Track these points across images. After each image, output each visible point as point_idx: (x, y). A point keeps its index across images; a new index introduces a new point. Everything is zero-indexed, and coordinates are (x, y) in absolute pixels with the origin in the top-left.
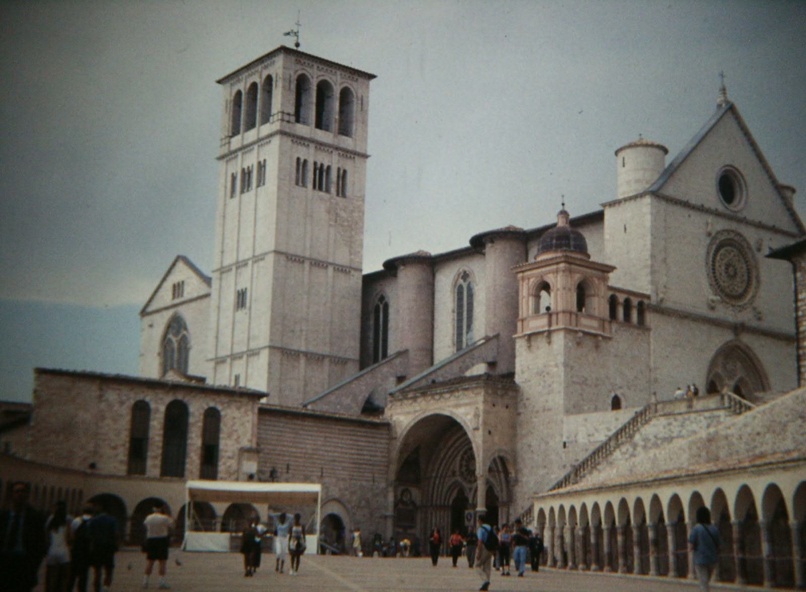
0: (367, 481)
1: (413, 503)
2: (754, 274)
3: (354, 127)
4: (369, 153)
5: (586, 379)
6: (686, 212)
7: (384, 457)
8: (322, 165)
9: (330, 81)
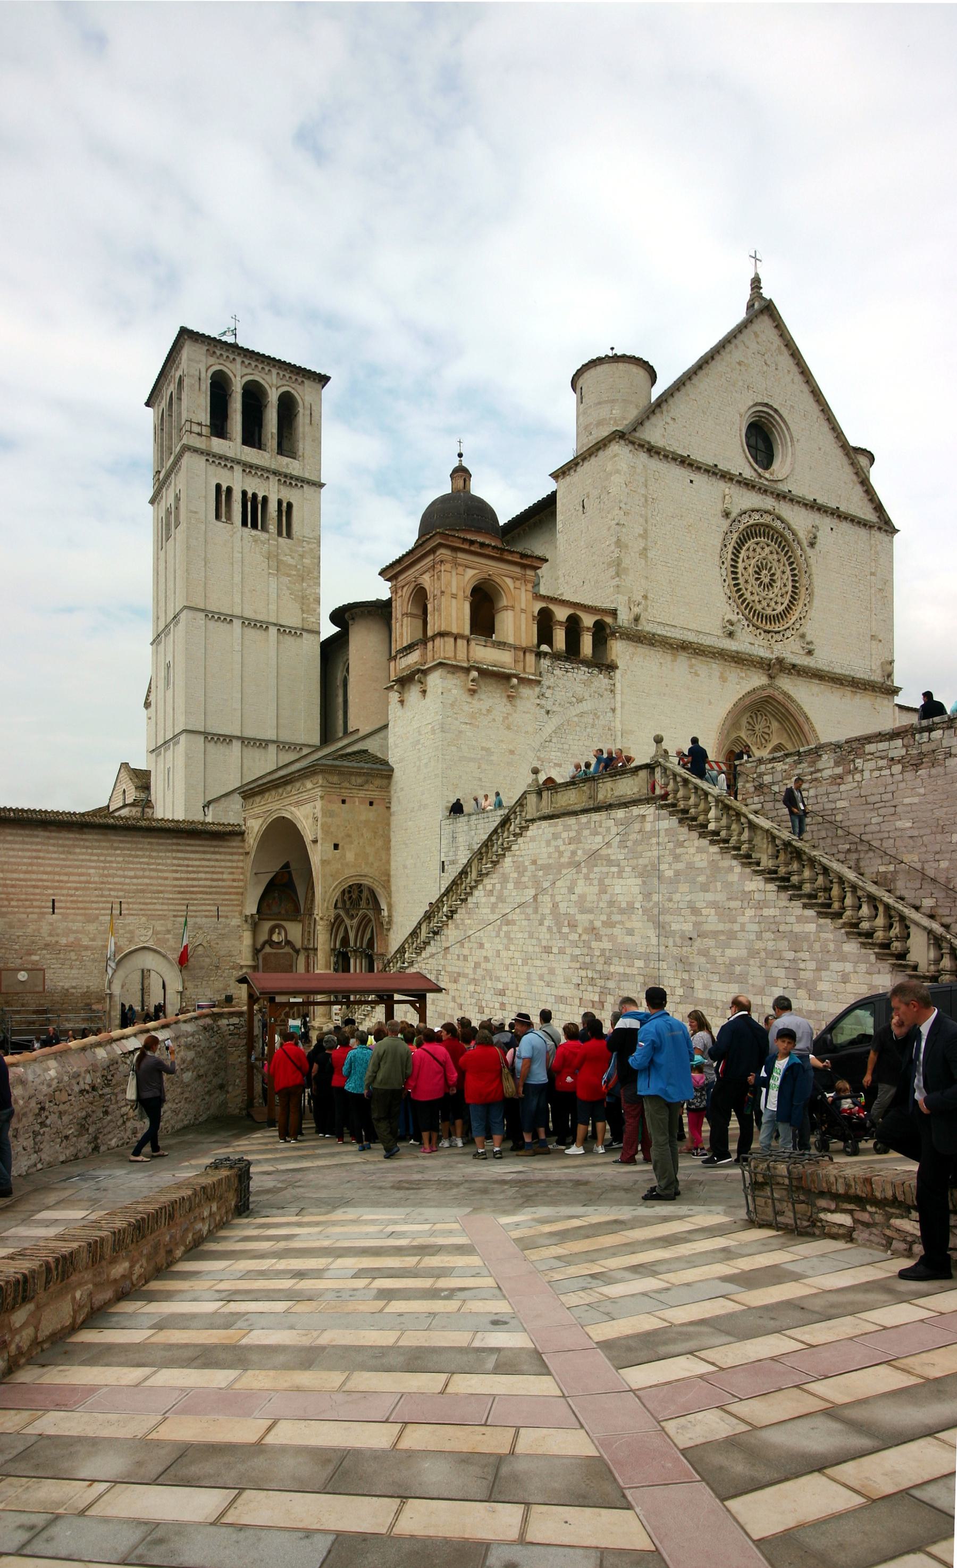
0: (206, 917)
1: (288, 943)
2: (804, 580)
3: (301, 445)
7: (234, 880)
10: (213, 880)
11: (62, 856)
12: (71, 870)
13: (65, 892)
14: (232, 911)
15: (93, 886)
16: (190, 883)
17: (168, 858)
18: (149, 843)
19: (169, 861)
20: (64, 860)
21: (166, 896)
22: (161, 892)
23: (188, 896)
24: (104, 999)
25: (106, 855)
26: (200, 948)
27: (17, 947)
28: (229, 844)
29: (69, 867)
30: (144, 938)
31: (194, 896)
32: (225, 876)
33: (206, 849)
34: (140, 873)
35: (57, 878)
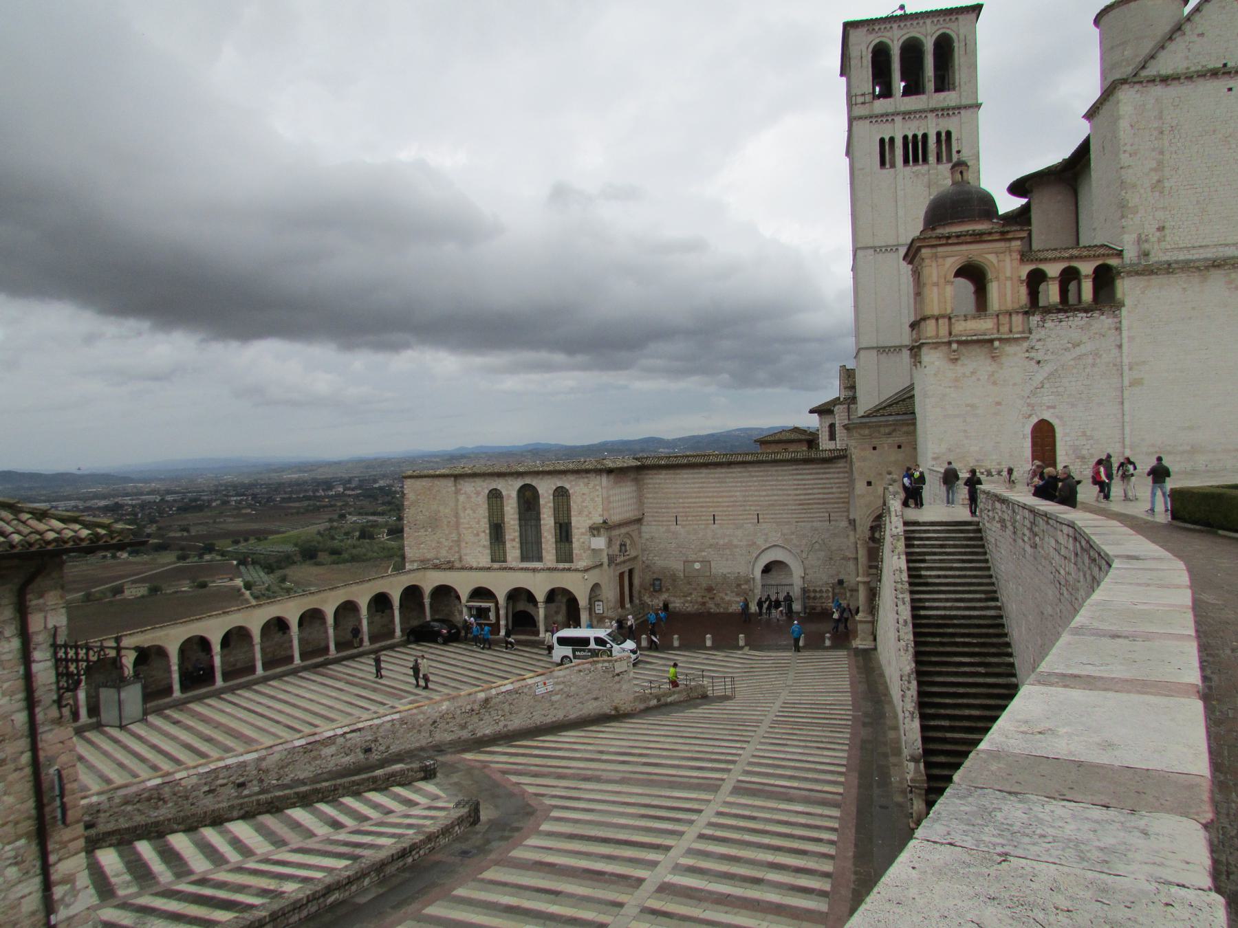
0: (820, 521)
4: (979, 102)
5: (972, 406)
6: (1221, 84)
7: (841, 493)
8: (915, 136)
9: (918, 35)
10: (824, 494)
11: (718, 485)
12: (724, 494)
13: (720, 509)
14: (841, 516)
15: (737, 504)
16: (807, 497)
17: (790, 480)
18: (776, 471)
19: (791, 483)
20: (718, 487)
21: (790, 507)
22: (786, 505)
23: (805, 507)
24: (749, 581)
25: (747, 482)
26: (817, 544)
27: (693, 547)
28: (836, 465)
29: (722, 492)
30: (775, 538)
31: (810, 507)
32: (834, 490)
33: (818, 471)
34: (770, 493)
35: (715, 500)
